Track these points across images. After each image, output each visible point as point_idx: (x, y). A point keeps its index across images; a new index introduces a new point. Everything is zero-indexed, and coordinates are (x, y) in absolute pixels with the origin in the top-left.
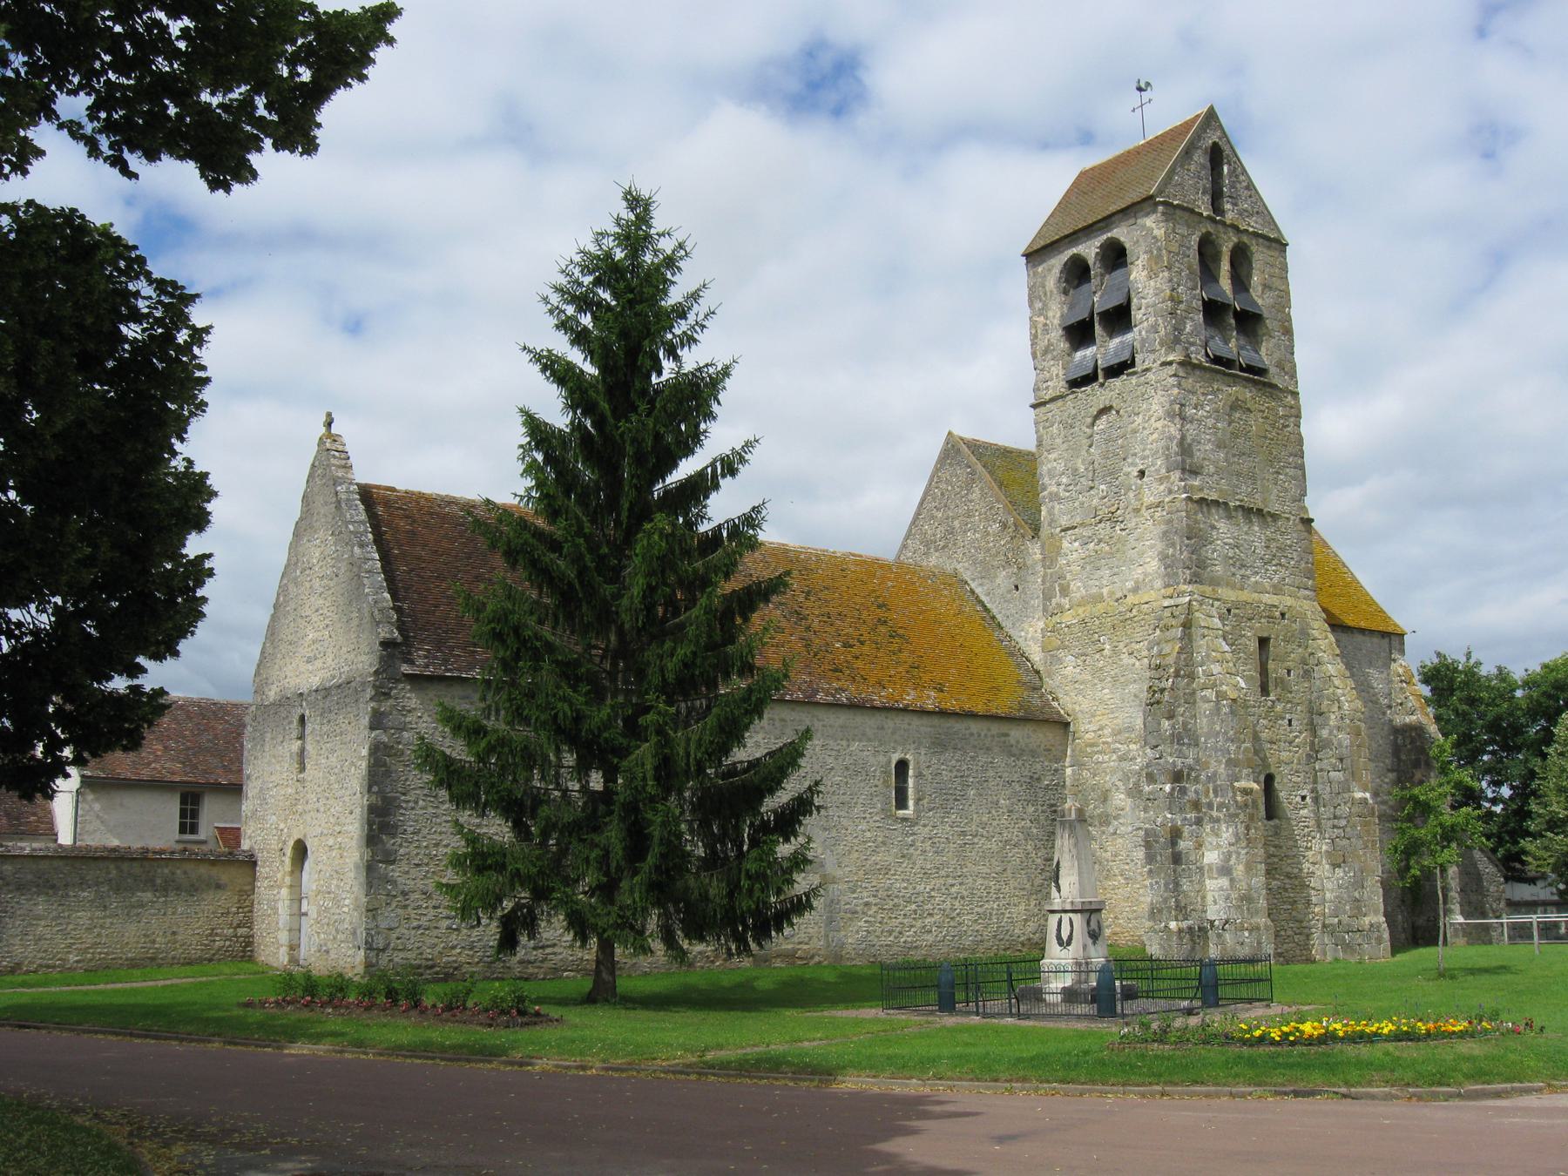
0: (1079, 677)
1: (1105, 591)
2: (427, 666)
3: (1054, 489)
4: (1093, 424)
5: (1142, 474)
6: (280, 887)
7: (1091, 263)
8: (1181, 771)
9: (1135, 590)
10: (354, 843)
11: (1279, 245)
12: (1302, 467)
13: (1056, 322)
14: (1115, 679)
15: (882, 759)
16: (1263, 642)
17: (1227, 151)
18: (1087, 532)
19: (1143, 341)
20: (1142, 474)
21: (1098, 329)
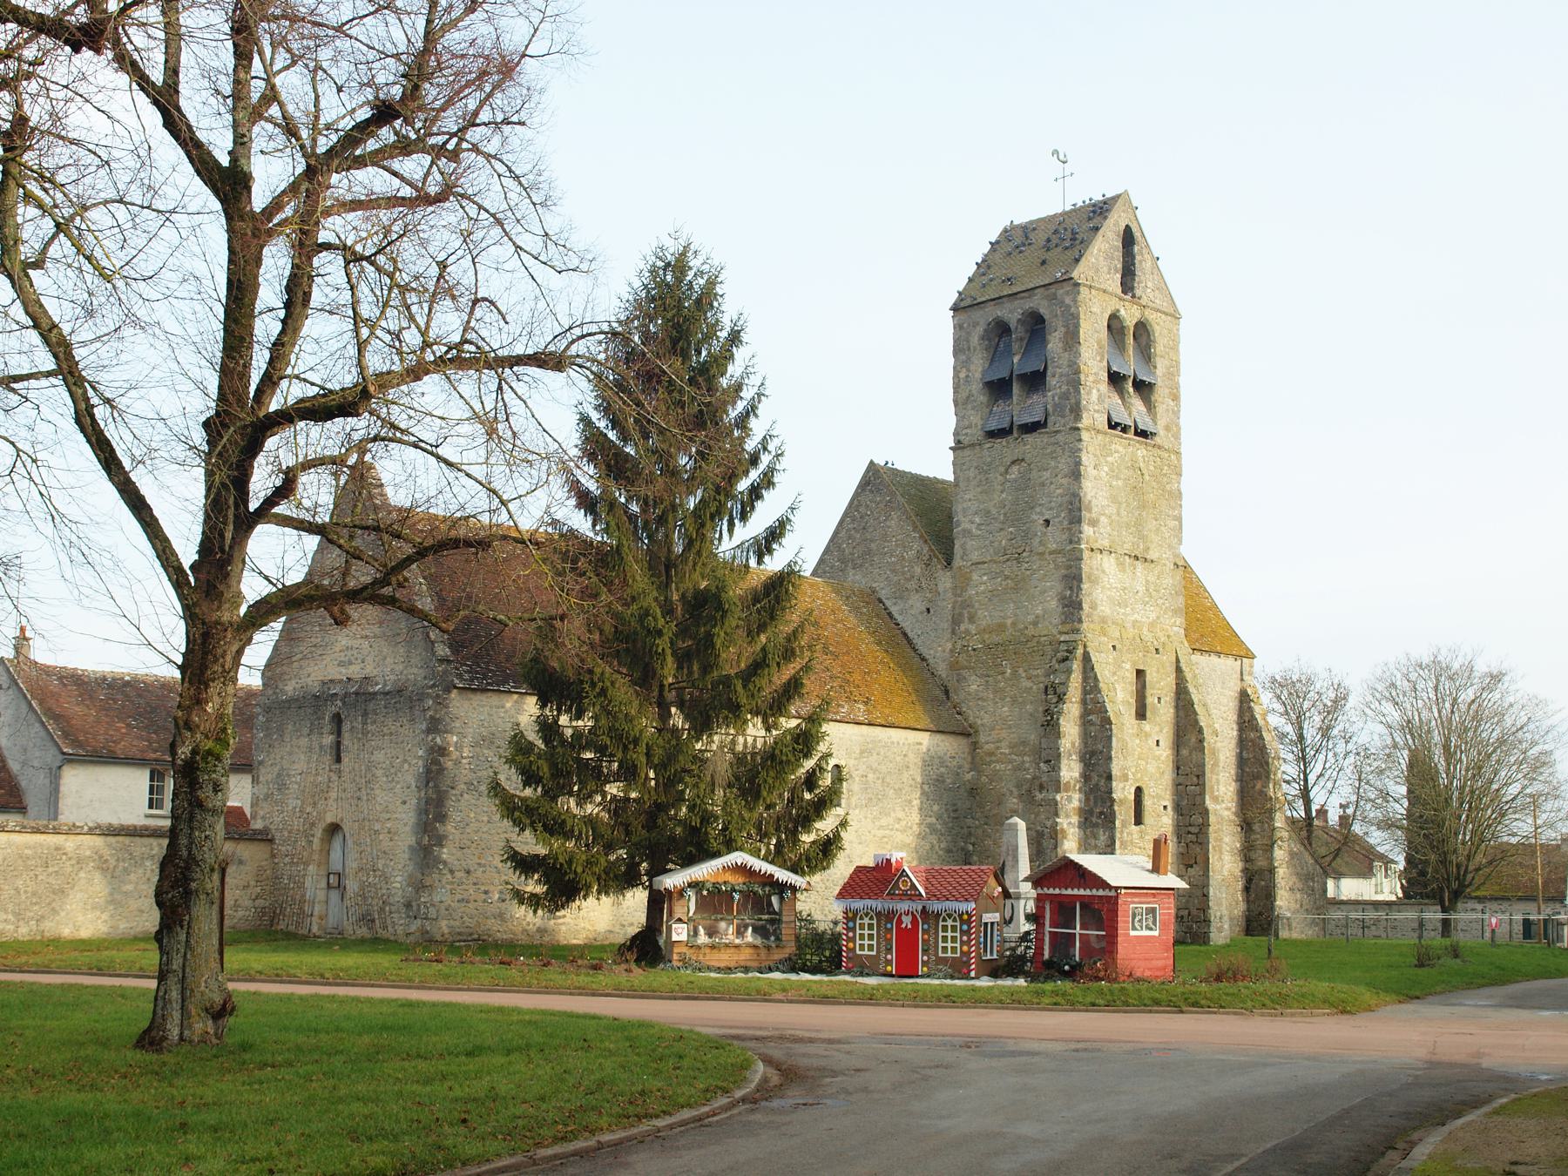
2: (472, 680)
4: (1007, 472)
5: (1047, 522)
9: (1035, 624)
10: (408, 828)
11: (1175, 316)
12: (1179, 519)
13: (978, 375)
14: (1014, 701)
16: (1140, 673)
17: (1137, 234)
19: (1055, 406)
20: (1047, 522)
21: (1016, 389)
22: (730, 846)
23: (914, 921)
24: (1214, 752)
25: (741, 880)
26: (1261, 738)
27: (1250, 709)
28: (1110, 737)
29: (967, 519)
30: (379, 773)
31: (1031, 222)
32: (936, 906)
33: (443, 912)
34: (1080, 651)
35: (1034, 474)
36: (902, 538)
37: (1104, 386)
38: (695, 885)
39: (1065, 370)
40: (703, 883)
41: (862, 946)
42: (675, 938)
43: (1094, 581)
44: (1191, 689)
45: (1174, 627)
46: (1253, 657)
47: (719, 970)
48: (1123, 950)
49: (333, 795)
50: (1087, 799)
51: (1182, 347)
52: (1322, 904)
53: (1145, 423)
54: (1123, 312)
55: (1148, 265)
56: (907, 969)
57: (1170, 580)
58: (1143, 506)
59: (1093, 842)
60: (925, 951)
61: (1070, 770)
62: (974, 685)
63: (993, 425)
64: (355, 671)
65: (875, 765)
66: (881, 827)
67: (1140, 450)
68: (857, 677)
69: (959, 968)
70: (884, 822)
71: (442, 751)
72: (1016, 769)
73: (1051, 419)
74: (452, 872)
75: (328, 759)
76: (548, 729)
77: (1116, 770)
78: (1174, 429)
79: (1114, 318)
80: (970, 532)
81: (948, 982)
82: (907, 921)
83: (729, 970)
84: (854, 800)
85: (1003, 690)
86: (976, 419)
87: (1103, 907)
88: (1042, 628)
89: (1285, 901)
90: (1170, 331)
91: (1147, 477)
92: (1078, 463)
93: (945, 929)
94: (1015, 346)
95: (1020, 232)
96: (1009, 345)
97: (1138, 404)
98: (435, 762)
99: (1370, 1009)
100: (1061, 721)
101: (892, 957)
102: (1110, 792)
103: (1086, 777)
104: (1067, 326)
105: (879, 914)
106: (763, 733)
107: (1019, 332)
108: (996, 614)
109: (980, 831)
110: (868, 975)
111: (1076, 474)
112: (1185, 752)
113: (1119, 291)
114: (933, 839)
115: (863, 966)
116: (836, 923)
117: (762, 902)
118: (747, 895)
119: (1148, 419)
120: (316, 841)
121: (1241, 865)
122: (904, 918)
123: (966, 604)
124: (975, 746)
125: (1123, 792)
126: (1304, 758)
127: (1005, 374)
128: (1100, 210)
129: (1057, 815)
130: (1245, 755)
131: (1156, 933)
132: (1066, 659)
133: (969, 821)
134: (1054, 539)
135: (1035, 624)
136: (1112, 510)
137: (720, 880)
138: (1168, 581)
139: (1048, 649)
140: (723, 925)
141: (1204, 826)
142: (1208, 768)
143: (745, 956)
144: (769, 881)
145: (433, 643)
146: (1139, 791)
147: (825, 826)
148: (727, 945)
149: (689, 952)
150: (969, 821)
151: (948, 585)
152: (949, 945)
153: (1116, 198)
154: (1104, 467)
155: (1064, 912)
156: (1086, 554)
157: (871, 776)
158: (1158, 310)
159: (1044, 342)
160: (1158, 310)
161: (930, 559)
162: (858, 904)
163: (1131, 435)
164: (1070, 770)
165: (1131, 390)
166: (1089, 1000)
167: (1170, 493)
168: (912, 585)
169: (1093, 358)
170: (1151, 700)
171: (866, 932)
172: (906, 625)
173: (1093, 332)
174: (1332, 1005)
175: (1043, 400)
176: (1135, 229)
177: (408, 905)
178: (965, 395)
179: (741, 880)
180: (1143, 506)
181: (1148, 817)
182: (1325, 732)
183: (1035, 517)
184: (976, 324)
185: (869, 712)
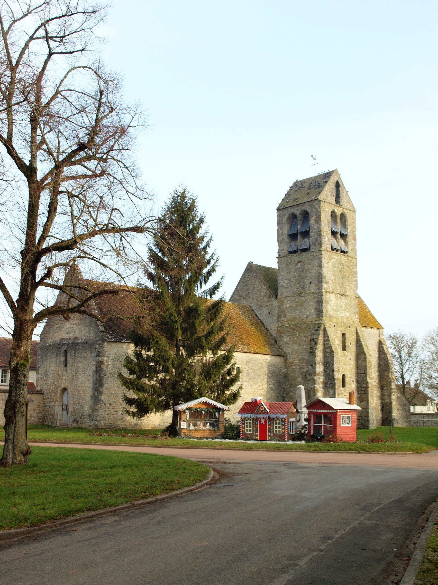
0: (288, 342)
1: (297, 317)
2: (112, 338)
3: (283, 284)
4: (296, 265)
6: (55, 402)
9: (307, 318)
10: (90, 389)
11: (354, 211)
12: (356, 281)
13: (286, 232)
14: (299, 345)
16: (344, 335)
17: (341, 184)
18: (292, 298)
19: (313, 243)
20: (310, 283)
21: (299, 237)
22: (201, 395)
24: (370, 362)
25: (205, 407)
26: (386, 357)
27: (382, 347)
28: (333, 357)
29: (282, 282)
30: (80, 370)
31: (304, 180)
32: (273, 416)
33: (102, 418)
34: (322, 327)
36: (261, 289)
37: (330, 236)
38: (189, 409)
39: (316, 230)
40: (192, 408)
41: (247, 430)
42: (182, 427)
43: (327, 303)
44: (362, 340)
45: (355, 318)
46: (383, 329)
47: (197, 438)
48: (339, 431)
49: (64, 378)
50: (326, 379)
51: (357, 222)
52: (409, 415)
53: (344, 248)
54: (336, 210)
55: (344, 194)
56: (263, 438)
57: (354, 302)
58: (344, 277)
59: (328, 393)
60: (269, 432)
61: (319, 369)
63: (291, 249)
64: (72, 335)
65: (251, 367)
66: (254, 388)
67: (343, 258)
68: (245, 336)
69: (281, 438)
71: (102, 363)
72: (300, 368)
73: (311, 247)
74: (105, 404)
75: (62, 366)
76: (138, 355)
77: (335, 368)
78: (354, 250)
79: (333, 212)
80: (283, 286)
81: (278, 442)
82: (263, 421)
83: (201, 438)
84: (244, 379)
85: (296, 341)
86: (285, 247)
87: (332, 416)
88: (309, 319)
89: (396, 414)
91: (345, 267)
92: (321, 262)
93: (276, 424)
94: (299, 222)
95: (300, 183)
96: (297, 220)
97: (342, 242)
98: (99, 366)
99: (426, 452)
100: (316, 351)
101: (258, 433)
102: (333, 376)
103: (325, 371)
104: (316, 215)
105: (253, 419)
106: (212, 356)
107: (300, 217)
108: (293, 314)
109: (288, 390)
110: (249, 440)
112: (360, 362)
113: (334, 203)
114: (272, 392)
115: (248, 437)
116: (238, 422)
117: (212, 415)
118: (207, 412)
119: (345, 247)
120: (58, 394)
121: (380, 401)
122: (262, 420)
123: (283, 311)
124: (286, 360)
125: (338, 376)
126: (401, 364)
127: (295, 232)
128: (327, 176)
129: (315, 384)
130: (381, 363)
131: (350, 425)
132: (317, 330)
133: (284, 386)
135: (307, 318)
136: (333, 278)
137: (198, 407)
139: (311, 326)
140: (199, 423)
141: (367, 387)
142: (368, 367)
143: (207, 433)
144: (215, 407)
145: (98, 326)
146: (344, 376)
147: (234, 388)
148: (200, 430)
149: (187, 432)
150: (284, 386)
151: (276, 305)
152: (278, 429)
153: (333, 171)
154: (330, 264)
155: (318, 418)
156: (324, 294)
157: (250, 371)
159: (309, 221)
160: (348, 210)
161: (270, 296)
162: (246, 415)
163: (339, 252)
164: (319, 369)
165: (339, 237)
166: (327, 449)
167: (353, 272)
168: (264, 304)
169: (326, 226)
170: (347, 344)
171: (249, 425)
172: (262, 318)
173: (325, 217)
174: (413, 451)
175: (308, 240)
176: (340, 182)
177: (90, 416)
178: (281, 239)
180: (344, 277)
181: (347, 385)
182: (409, 354)
183: (306, 281)
184: (285, 215)
185: (249, 348)
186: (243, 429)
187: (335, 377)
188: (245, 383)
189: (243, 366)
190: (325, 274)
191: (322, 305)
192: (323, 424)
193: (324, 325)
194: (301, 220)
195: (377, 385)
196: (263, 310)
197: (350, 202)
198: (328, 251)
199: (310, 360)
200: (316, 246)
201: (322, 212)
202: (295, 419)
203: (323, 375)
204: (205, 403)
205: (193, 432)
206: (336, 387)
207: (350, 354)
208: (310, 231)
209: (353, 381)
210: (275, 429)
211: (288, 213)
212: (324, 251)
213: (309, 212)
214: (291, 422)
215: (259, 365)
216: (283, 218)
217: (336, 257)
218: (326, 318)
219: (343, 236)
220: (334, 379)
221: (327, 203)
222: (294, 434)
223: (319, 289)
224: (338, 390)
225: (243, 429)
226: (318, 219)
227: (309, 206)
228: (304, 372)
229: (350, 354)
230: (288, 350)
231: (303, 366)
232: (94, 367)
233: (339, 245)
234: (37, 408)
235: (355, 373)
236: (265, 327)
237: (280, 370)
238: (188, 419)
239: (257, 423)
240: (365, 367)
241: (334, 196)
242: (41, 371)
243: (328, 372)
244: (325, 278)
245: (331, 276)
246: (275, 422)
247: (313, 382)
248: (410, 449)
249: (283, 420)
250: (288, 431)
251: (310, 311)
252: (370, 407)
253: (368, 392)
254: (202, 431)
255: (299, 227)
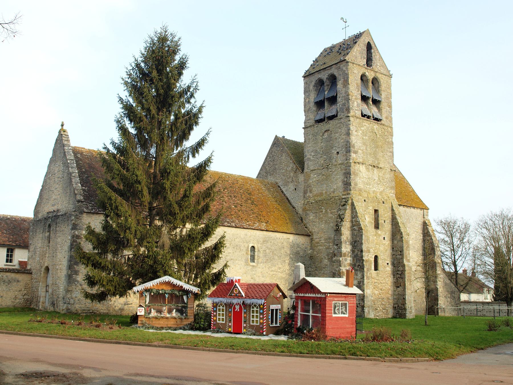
2: (92, 209)
3: (309, 157)
5: (338, 153)
7: (325, 81)
8: (345, 253)
9: (334, 192)
12: (392, 152)
13: (313, 100)
14: (326, 222)
15: (246, 246)
16: (376, 211)
18: (319, 172)
20: (338, 153)
21: (326, 104)
23: (240, 308)
24: (407, 242)
25: (169, 289)
26: (431, 239)
28: (362, 235)
29: (309, 154)
32: (248, 301)
33: (77, 301)
34: (350, 202)
35: (333, 135)
36: (287, 163)
37: (359, 101)
38: (147, 290)
39: (344, 95)
41: (219, 320)
43: (356, 175)
44: (398, 217)
45: (391, 194)
46: (428, 209)
47: (157, 329)
49: (47, 255)
50: (353, 260)
52: (457, 302)
53: (377, 115)
54: (367, 73)
56: (237, 331)
57: (389, 176)
58: (377, 147)
60: (245, 322)
61: (346, 248)
62: (311, 217)
63: (318, 118)
64: (55, 208)
65: (269, 247)
66: (272, 271)
67: (375, 126)
69: (258, 331)
70: (273, 268)
72: (326, 249)
74: (81, 285)
76: (106, 227)
77: (364, 248)
78: (390, 118)
80: (310, 159)
84: (260, 260)
85: (322, 218)
87: (321, 302)
88: (336, 194)
89: (443, 302)
90: (387, 82)
92: (349, 129)
93: (253, 312)
94: (326, 88)
99: (452, 357)
100: (342, 229)
103: (353, 251)
104: (344, 78)
107: (327, 83)
109: (314, 273)
111: (348, 134)
112: (395, 242)
118: (171, 295)
119: (378, 114)
122: (236, 306)
124: (312, 240)
125: (368, 257)
126: (453, 250)
127: (322, 98)
128: (358, 37)
129: (340, 266)
131: (347, 316)
132: (345, 205)
134: (340, 159)
135: (334, 192)
138: (388, 176)
141: (404, 271)
142: (405, 248)
143: (171, 323)
145: (76, 194)
146: (376, 257)
148: (162, 318)
151: (302, 179)
152: (255, 319)
154: (359, 132)
156: (352, 164)
158: (382, 74)
159: (336, 85)
160: (382, 74)
162: (217, 300)
165: (371, 103)
166: (299, 350)
167: (388, 142)
168: (290, 180)
169: (355, 90)
170: (381, 221)
172: (288, 195)
174: (430, 355)
176: (372, 43)
178: (308, 108)
179: (169, 289)
180: (377, 147)
181: (380, 267)
182: (461, 240)
183: (333, 151)
185: (267, 226)
186: (215, 318)
187: (364, 258)
188: (262, 264)
189: (259, 245)
190: (353, 142)
191: (350, 177)
192: (311, 314)
193: (352, 200)
194: (328, 85)
195: (419, 268)
196: (289, 186)
197: (384, 66)
198: (357, 118)
199: (335, 239)
200: (343, 112)
201: (350, 74)
202: (280, 306)
203: (350, 256)
204: (168, 283)
205: (154, 320)
206: (365, 269)
207: (384, 233)
208: (338, 97)
209: (388, 264)
210: (251, 319)
211: (314, 79)
212: (352, 117)
213: (337, 76)
214: (272, 310)
215: (279, 244)
216: (309, 85)
217: (367, 125)
218: (355, 192)
219: (376, 102)
220: (363, 260)
221: (356, 64)
222: (278, 325)
223: (347, 160)
224: (367, 273)
225: (215, 318)
226: (346, 83)
227: (336, 69)
228: (330, 253)
229: (384, 233)
230: (314, 228)
231: (329, 246)
232: (69, 242)
233: (371, 112)
234: (23, 289)
235: (390, 254)
236: (291, 204)
237: (305, 251)
238: (147, 303)
239: (230, 310)
240: (402, 247)
241: (364, 58)
242: (32, 248)
243: (356, 253)
244: (354, 147)
245: (361, 145)
246: (252, 309)
247: (339, 264)
248: (426, 353)
249: (262, 306)
250: (268, 321)
251: (338, 184)
252: (407, 293)
253: (405, 276)
254: (165, 320)
255: (326, 93)
